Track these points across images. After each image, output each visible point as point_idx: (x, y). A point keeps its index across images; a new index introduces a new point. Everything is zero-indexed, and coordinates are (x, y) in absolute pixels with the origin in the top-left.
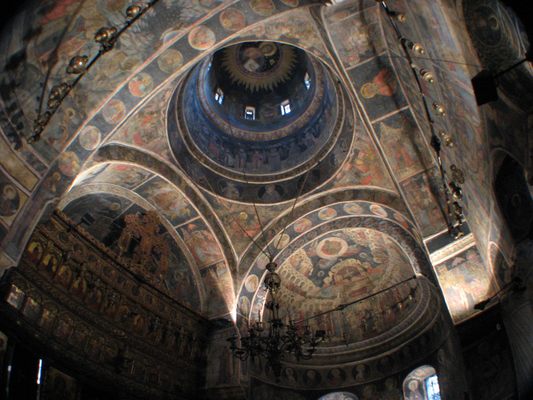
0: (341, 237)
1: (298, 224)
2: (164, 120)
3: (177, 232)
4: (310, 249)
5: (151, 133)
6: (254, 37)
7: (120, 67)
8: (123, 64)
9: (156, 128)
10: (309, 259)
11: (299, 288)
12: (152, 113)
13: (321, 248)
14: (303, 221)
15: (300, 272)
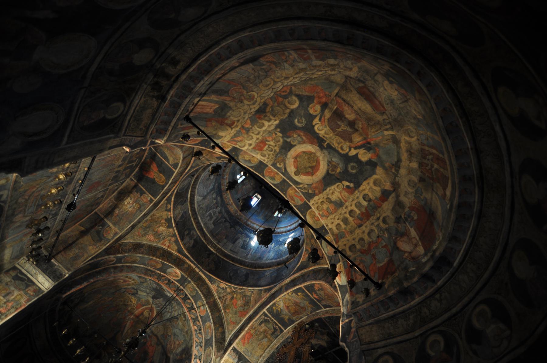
0: (284, 161)
1: (294, 201)
2: (242, 289)
3: (328, 309)
4: (310, 192)
5: (245, 301)
6: (176, 242)
7: (185, 321)
8: (184, 319)
9: (245, 296)
10: (328, 189)
11: (371, 203)
12: (232, 298)
13: (310, 177)
14: (290, 196)
15: (346, 201)
